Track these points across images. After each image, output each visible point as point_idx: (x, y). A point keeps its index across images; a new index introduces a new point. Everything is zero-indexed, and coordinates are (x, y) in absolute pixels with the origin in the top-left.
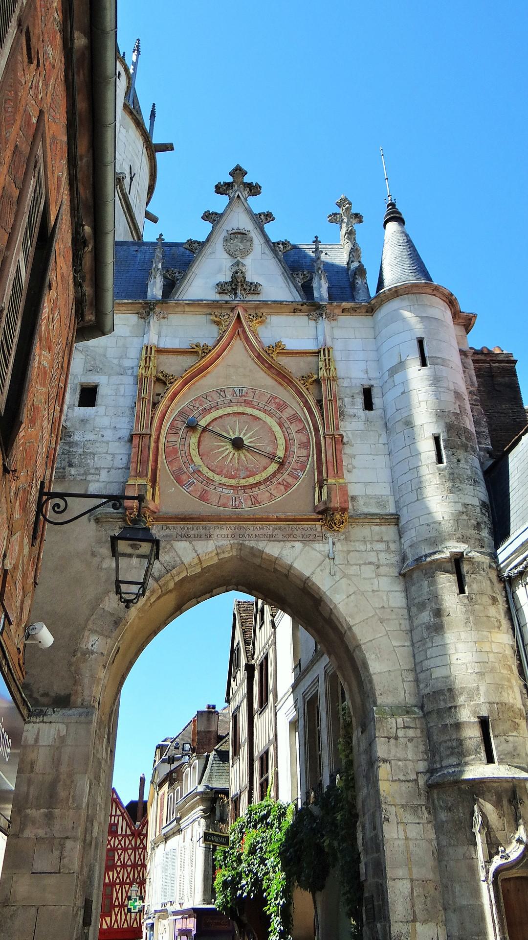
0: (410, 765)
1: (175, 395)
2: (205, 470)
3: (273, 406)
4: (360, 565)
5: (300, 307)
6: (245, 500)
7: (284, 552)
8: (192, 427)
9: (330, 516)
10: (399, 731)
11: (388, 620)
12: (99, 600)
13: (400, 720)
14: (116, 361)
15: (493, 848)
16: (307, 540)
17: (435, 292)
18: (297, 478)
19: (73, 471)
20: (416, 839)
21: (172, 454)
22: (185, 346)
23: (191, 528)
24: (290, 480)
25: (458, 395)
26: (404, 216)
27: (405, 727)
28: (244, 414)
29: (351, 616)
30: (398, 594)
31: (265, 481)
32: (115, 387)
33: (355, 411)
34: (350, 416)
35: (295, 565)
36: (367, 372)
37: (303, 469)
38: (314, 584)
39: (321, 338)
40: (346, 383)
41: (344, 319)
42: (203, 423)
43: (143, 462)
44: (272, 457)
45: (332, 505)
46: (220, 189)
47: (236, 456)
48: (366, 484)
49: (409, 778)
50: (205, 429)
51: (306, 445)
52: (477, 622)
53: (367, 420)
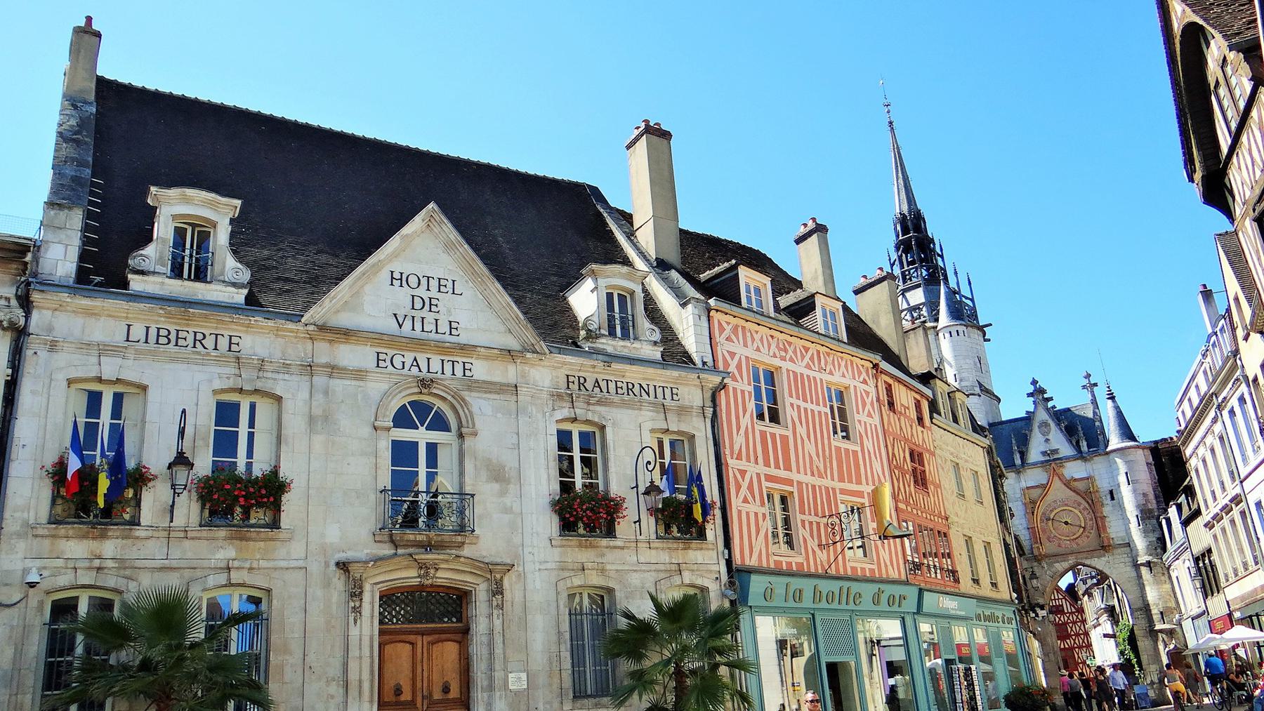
9: (1105, 547)
15: (1166, 646)
21: (1044, 531)
46: (1030, 395)
52: (1157, 582)
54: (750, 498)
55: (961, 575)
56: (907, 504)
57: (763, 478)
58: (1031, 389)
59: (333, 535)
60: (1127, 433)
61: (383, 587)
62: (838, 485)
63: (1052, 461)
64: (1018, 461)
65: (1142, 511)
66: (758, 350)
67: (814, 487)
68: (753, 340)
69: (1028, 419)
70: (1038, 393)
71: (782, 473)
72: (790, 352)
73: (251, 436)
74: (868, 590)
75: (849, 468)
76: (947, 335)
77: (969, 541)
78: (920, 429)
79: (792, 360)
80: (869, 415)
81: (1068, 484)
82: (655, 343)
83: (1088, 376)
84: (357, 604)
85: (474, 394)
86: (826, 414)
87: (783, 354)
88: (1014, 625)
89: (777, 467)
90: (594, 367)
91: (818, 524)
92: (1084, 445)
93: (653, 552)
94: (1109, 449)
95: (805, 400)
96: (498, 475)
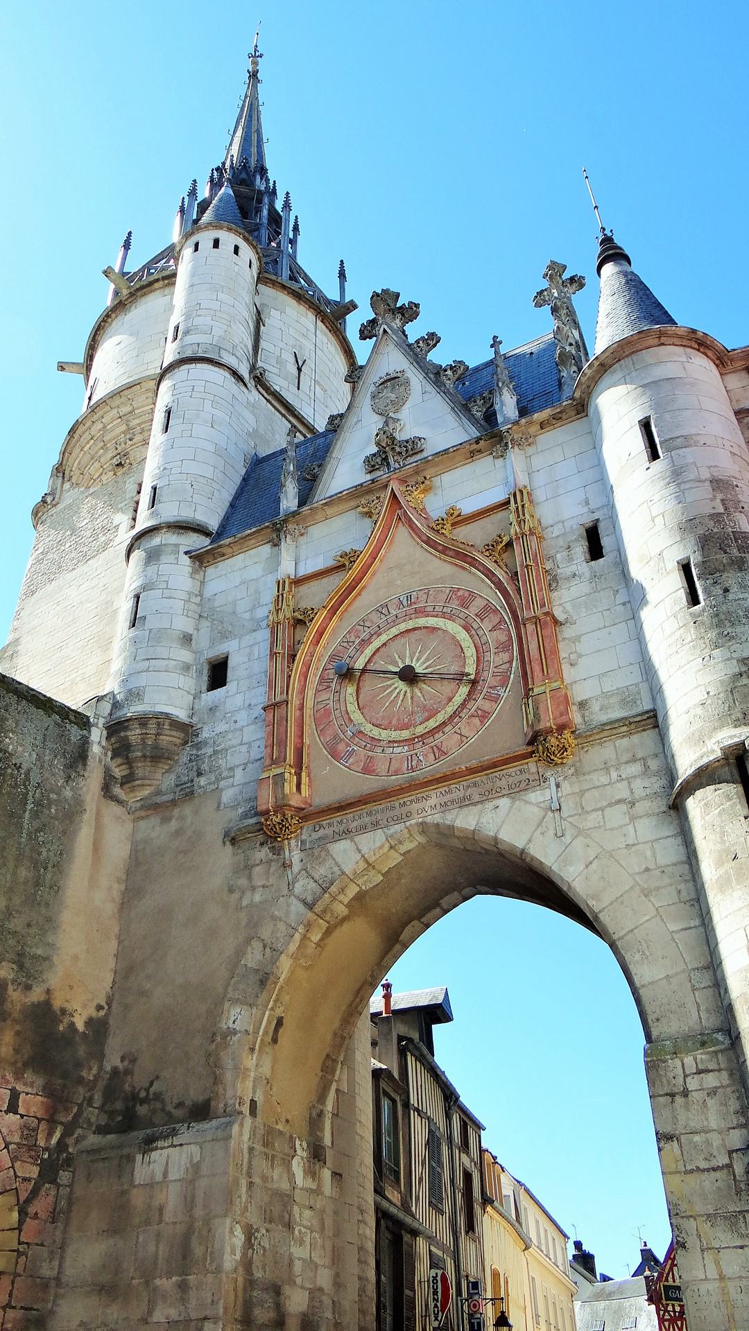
0: (716, 1139)
1: (320, 634)
2: (368, 728)
3: (455, 604)
4: (602, 809)
5: (475, 447)
6: (425, 756)
7: (484, 820)
8: (347, 674)
9: (543, 746)
10: (688, 1080)
11: (657, 889)
12: (239, 953)
13: (689, 1060)
14: (247, 616)
16: (516, 791)
17: (663, 340)
18: (496, 699)
19: (203, 781)
20: (740, 1277)
21: (323, 718)
22: (331, 563)
23: (350, 819)
24: (487, 706)
26: (627, 252)
27: (699, 1072)
28: (415, 629)
29: (596, 897)
30: (672, 839)
31: (451, 718)
32: (247, 650)
33: (574, 568)
34: (567, 579)
35: (501, 836)
36: (587, 503)
37: (504, 683)
38: (533, 858)
39: (511, 479)
40: (557, 531)
41: (548, 438)
42: (359, 664)
43: (283, 743)
44: (460, 677)
45: (541, 726)
47: (409, 695)
48: (601, 676)
49: (714, 1163)
50: (364, 671)
51: (505, 647)
53: (594, 576)
65: (705, 542)
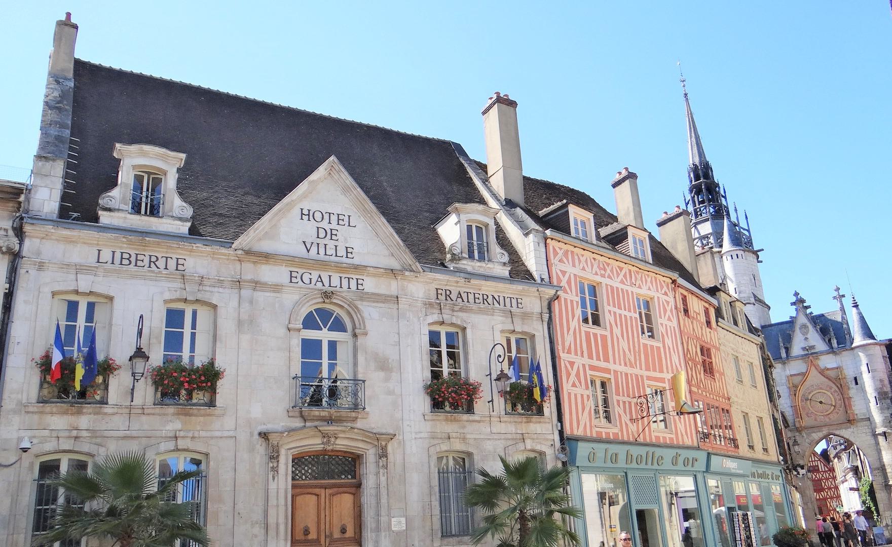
9: (850, 421)
16: (846, 428)
21: (804, 408)
23: (814, 429)
25: (881, 381)
46: (793, 304)
54: (577, 383)
55: (740, 443)
56: (699, 387)
57: (587, 368)
58: (794, 299)
59: (256, 411)
60: (868, 334)
61: (295, 451)
62: (645, 373)
63: (810, 354)
64: (784, 355)
66: (583, 269)
67: (626, 375)
68: (580, 261)
69: (792, 322)
70: (799, 302)
71: (602, 364)
72: (608, 271)
73: (193, 336)
74: (669, 454)
75: (654, 360)
76: (729, 258)
77: (746, 416)
78: (708, 330)
79: (609, 277)
80: (669, 319)
81: (822, 372)
82: (504, 264)
83: (838, 289)
84: (275, 465)
85: (365, 303)
86: (636, 318)
87: (603, 272)
88: (781, 481)
89: (598, 359)
90: (457, 282)
91: (630, 403)
92: (834, 342)
93: (503, 424)
94: (854, 345)
95: (620, 308)
96: (384, 365)
